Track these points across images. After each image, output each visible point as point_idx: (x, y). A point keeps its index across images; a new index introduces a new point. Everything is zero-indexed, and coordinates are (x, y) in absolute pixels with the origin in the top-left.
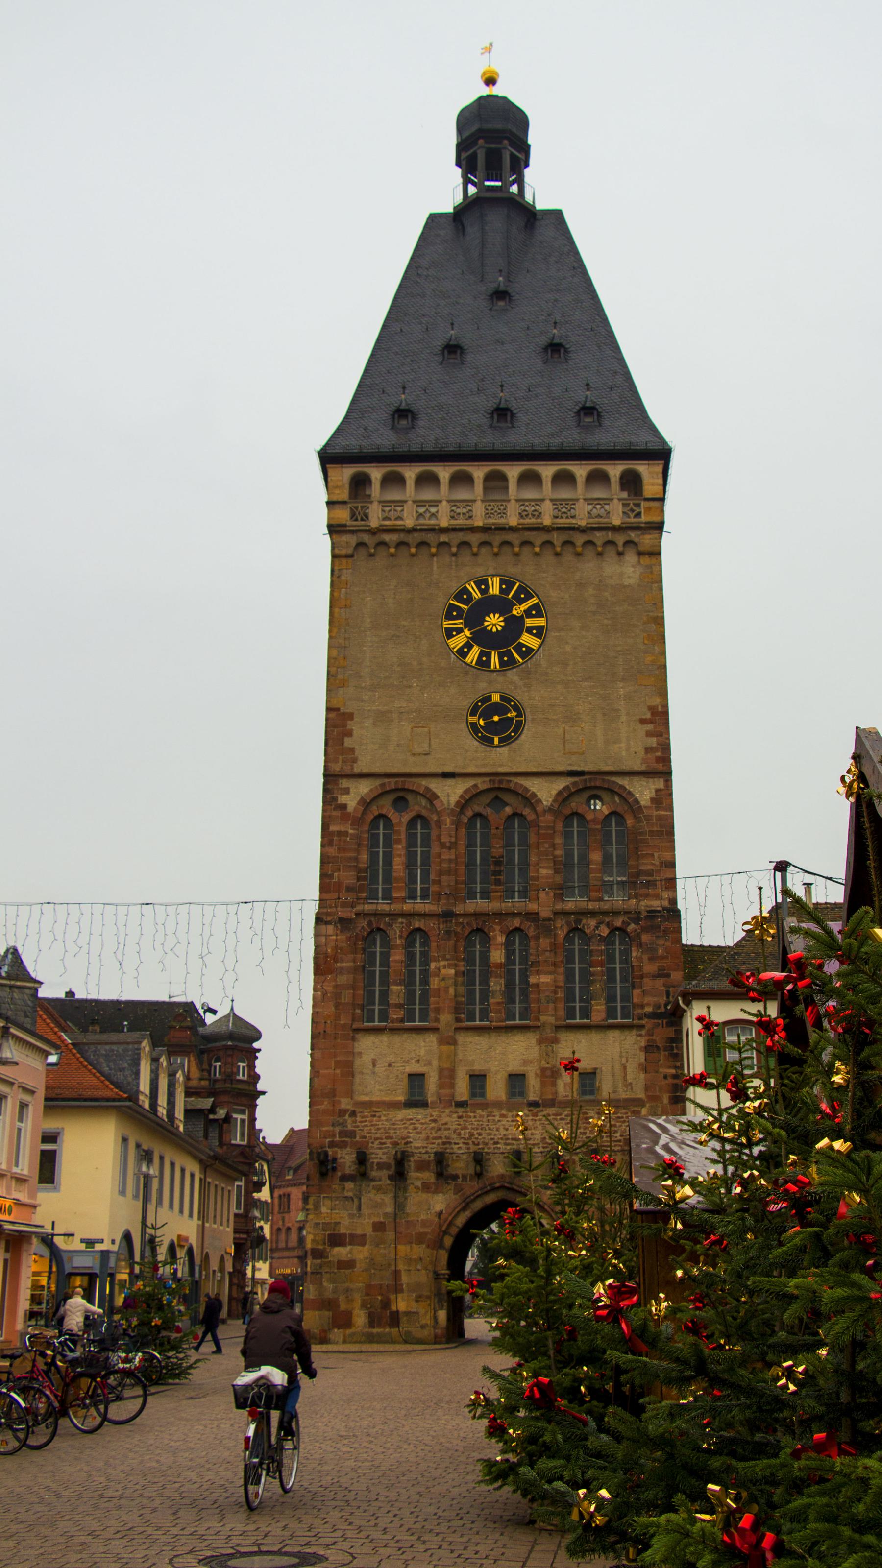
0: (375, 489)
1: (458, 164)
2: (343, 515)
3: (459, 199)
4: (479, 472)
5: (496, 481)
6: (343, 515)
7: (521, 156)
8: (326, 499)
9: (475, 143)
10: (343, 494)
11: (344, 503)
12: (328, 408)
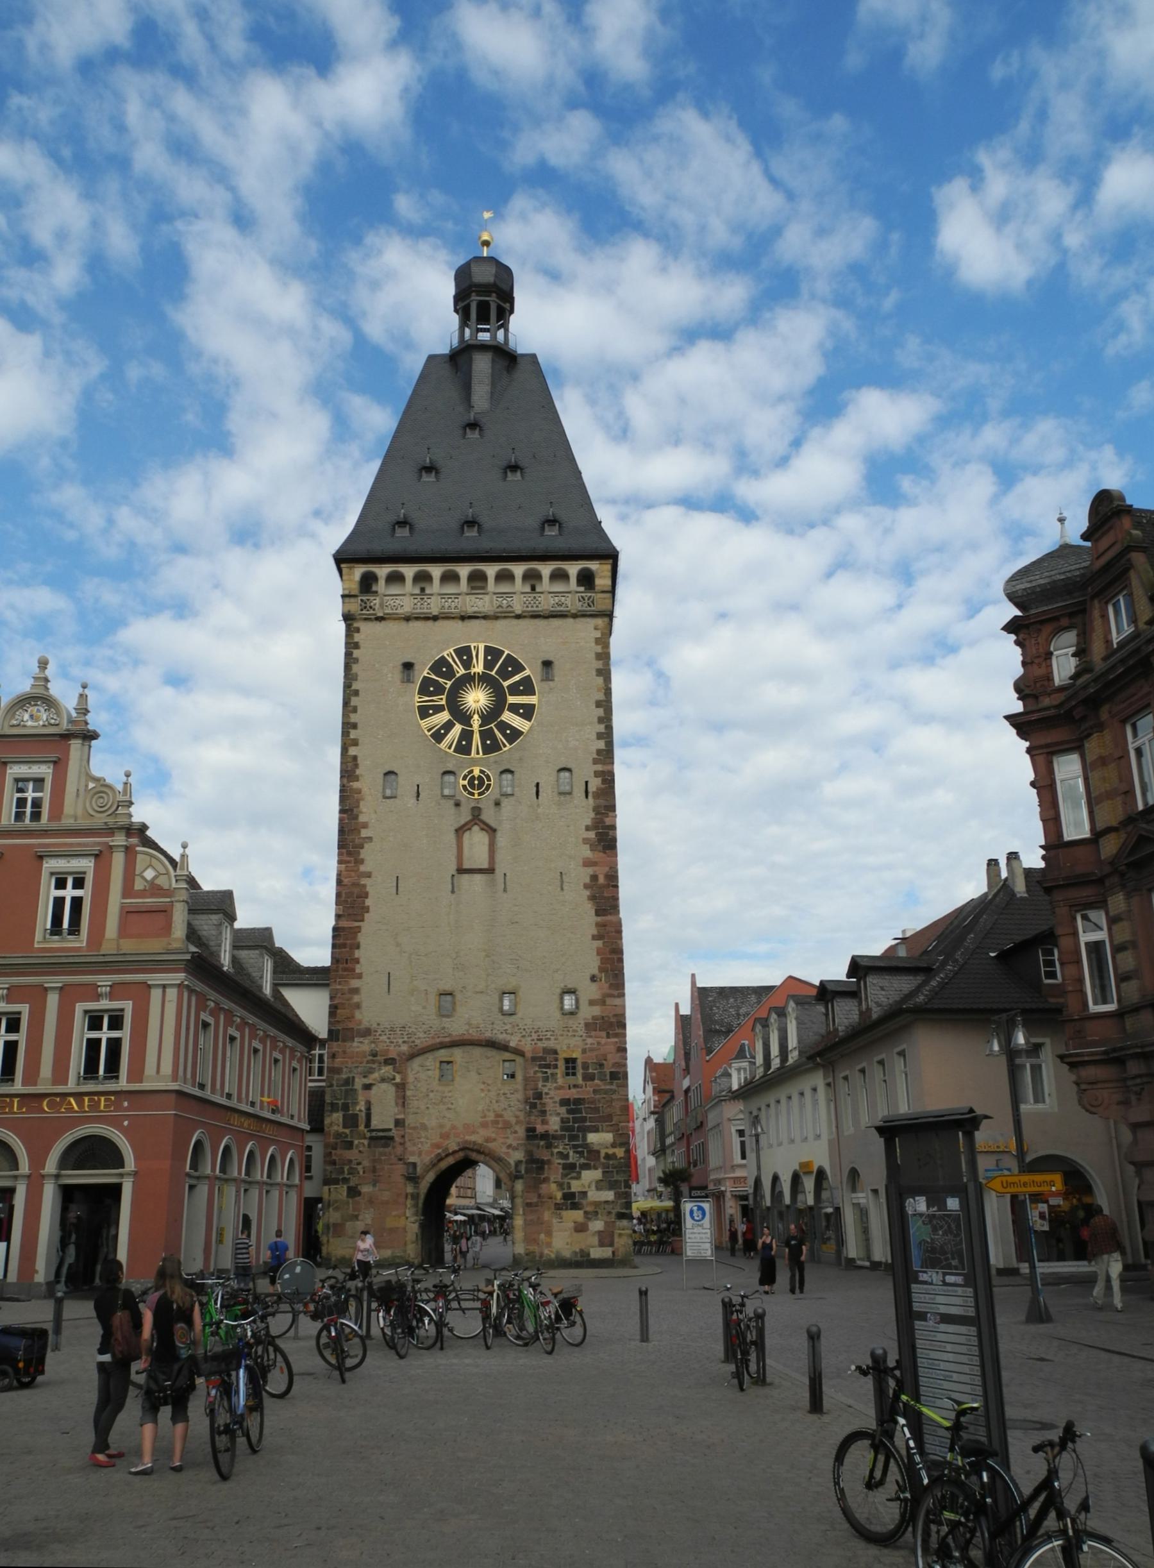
0: (381, 586)
1: (456, 311)
2: (354, 606)
3: (455, 343)
4: (464, 571)
5: (477, 578)
6: (354, 606)
7: (507, 306)
8: (341, 593)
9: (469, 296)
10: (355, 587)
11: (355, 596)
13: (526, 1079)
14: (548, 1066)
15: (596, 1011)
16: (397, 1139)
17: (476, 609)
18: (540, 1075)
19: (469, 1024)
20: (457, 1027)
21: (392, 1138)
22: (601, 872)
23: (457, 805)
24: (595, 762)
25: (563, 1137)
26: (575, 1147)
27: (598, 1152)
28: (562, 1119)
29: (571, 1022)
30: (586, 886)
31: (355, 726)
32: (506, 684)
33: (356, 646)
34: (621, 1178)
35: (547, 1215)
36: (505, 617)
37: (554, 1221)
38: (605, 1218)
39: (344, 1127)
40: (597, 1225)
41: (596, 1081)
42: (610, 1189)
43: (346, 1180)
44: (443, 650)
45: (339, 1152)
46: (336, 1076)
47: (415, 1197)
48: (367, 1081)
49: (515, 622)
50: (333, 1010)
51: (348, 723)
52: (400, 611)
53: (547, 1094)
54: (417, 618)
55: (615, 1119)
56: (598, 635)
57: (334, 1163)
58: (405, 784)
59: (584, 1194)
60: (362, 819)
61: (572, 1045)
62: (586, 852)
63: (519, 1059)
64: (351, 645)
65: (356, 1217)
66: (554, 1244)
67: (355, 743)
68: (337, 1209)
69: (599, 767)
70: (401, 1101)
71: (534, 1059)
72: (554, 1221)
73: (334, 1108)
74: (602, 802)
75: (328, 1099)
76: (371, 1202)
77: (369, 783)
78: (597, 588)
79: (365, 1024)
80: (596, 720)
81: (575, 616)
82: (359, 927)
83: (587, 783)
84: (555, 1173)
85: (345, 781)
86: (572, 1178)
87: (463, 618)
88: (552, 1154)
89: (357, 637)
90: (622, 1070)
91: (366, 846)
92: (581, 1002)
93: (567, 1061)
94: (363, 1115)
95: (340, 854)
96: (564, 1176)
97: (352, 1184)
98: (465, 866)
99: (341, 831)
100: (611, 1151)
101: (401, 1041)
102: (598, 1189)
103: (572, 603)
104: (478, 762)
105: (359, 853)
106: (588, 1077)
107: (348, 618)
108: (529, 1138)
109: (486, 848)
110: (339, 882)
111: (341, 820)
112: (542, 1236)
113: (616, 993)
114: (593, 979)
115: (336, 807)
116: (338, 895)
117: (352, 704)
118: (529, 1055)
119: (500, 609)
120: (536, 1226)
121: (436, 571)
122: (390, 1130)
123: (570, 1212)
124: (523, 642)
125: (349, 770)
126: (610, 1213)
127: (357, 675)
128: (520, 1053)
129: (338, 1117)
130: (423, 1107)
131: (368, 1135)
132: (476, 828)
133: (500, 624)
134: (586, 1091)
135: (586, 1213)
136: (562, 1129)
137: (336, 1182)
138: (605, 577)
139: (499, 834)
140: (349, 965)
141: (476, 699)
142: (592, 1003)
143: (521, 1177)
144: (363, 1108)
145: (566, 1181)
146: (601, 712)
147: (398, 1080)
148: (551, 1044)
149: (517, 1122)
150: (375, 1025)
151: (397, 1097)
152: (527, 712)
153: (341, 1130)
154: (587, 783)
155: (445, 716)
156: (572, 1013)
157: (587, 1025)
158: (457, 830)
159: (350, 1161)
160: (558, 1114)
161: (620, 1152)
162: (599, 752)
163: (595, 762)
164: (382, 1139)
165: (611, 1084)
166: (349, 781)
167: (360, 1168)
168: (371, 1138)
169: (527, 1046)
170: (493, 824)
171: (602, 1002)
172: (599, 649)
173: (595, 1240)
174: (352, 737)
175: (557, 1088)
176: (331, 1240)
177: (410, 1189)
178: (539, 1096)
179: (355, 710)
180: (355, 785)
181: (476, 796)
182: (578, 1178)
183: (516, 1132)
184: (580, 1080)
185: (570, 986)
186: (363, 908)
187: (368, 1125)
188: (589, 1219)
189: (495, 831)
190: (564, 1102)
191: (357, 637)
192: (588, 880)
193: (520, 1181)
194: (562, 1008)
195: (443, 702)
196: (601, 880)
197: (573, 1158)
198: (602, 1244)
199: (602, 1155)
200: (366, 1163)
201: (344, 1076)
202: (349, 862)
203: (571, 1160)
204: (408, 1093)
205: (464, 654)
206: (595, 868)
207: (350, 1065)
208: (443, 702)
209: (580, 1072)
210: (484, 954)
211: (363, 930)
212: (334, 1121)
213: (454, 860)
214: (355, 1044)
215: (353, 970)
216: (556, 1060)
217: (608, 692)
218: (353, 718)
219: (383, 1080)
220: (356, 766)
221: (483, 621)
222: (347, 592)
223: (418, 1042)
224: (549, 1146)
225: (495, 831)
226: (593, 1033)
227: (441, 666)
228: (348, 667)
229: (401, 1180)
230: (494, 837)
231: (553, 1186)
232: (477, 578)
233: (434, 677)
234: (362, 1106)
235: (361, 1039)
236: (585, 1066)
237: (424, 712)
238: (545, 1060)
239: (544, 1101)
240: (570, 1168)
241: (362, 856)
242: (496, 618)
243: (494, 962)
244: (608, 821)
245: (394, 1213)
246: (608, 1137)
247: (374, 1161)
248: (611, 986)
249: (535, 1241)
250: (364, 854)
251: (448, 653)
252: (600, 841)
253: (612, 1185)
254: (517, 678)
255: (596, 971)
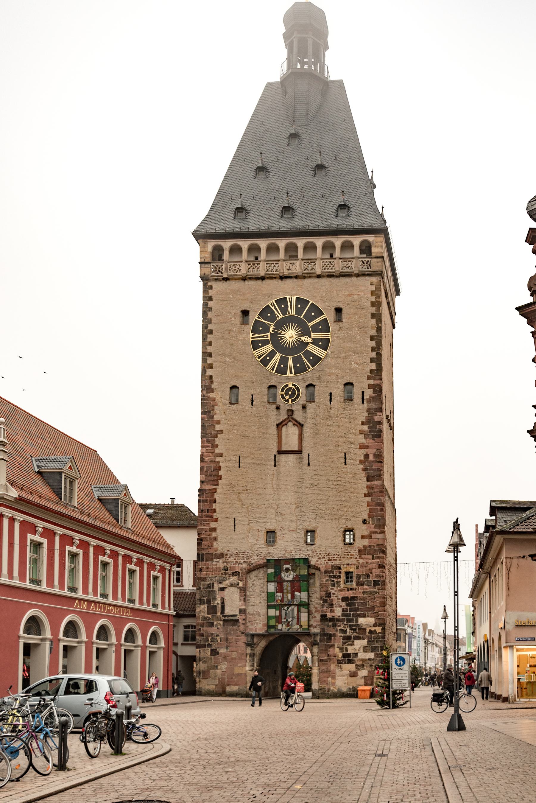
0: (226, 256)
2: (209, 270)
4: (282, 243)
5: (291, 249)
6: (209, 270)
12: (198, 207)
13: (321, 585)
14: (335, 577)
15: (366, 542)
16: (240, 621)
17: (289, 271)
18: (330, 582)
19: (286, 551)
20: (277, 552)
21: (237, 621)
22: (371, 452)
23: (278, 408)
24: (369, 378)
25: (343, 620)
26: (350, 626)
27: (365, 629)
28: (343, 610)
29: (349, 549)
30: (361, 462)
31: (210, 355)
32: (310, 324)
33: (211, 299)
34: (379, 645)
35: (333, 667)
36: (310, 277)
37: (337, 670)
38: (368, 668)
39: (208, 614)
40: (363, 673)
41: (365, 586)
42: (372, 652)
43: (210, 645)
44: (268, 301)
45: (205, 628)
46: (202, 583)
47: (252, 655)
48: (222, 586)
49: (317, 280)
50: (200, 542)
51: (206, 353)
52: (239, 273)
53: (334, 594)
54: (251, 279)
55: (376, 609)
56: (373, 288)
57: (202, 635)
58: (244, 395)
59: (356, 654)
60: (216, 418)
61: (350, 563)
62: (362, 439)
63: (317, 573)
64: (207, 299)
65: (216, 667)
66: (337, 683)
67: (211, 367)
68: (204, 662)
69: (371, 382)
70: (242, 598)
71: (326, 572)
72: (337, 670)
73: (201, 602)
74: (373, 406)
75: (198, 597)
76: (225, 658)
77: (221, 394)
78: (372, 254)
79: (220, 551)
80: (370, 349)
81: (357, 275)
82: (216, 489)
83: (363, 392)
84: (338, 641)
85: (205, 392)
86: (348, 645)
87: (282, 278)
88: (336, 631)
89: (211, 293)
90: (382, 579)
91: (219, 436)
92: (356, 536)
93: (347, 573)
94: (220, 606)
95: (202, 442)
96: (344, 643)
97: (213, 648)
98: (284, 449)
99: (203, 426)
100: (373, 629)
101: (242, 561)
102: (364, 651)
103: (356, 266)
104: (291, 380)
105: (214, 441)
106: (359, 584)
107: (204, 278)
108: (322, 620)
109: (296, 438)
110: (202, 460)
111: (202, 418)
112: (330, 679)
113: (378, 531)
114: (364, 522)
115: (200, 411)
116: (202, 468)
117: (208, 340)
118: (323, 570)
119: (306, 271)
120: (326, 673)
121: (263, 244)
122: (236, 615)
123: (347, 665)
124: (323, 295)
125: (207, 385)
126: (371, 666)
127: (211, 320)
128: (318, 569)
129: (204, 608)
130: (258, 602)
131: (223, 618)
132: (290, 424)
133: (307, 282)
134: (359, 592)
135: (356, 665)
136: (343, 615)
137: (204, 646)
138: (378, 246)
139: (305, 428)
140: (209, 513)
141: (290, 335)
142: (363, 537)
143: (317, 644)
144: (219, 602)
145: (345, 646)
146: (373, 344)
147: (241, 585)
148: (337, 563)
149: (315, 612)
150: (226, 551)
151: (241, 596)
152: (325, 344)
153: (206, 615)
154: (363, 392)
155: (269, 348)
156: (350, 544)
157: (360, 551)
158: (278, 425)
159: (212, 634)
160: (341, 606)
161: (379, 629)
162: (371, 371)
163: (369, 378)
164: (232, 621)
165: (374, 587)
166: (207, 393)
167: (218, 638)
168: (225, 621)
169: (322, 563)
170: (301, 422)
171: (370, 537)
172: (373, 299)
173: (362, 681)
174: (208, 362)
175: (340, 591)
176: (202, 680)
177: (249, 651)
178: (329, 595)
179: (210, 344)
180: (211, 395)
181: (290, 403)
182: (352, 645)
183: (315, 617)
184: (355, 586)
185: (349, 527)
186: (218, 477)
187: (223, 612)
188: (359, 669)
189: (302, 425)
190: (344, 599)
191: (211, 293)
192: (362, 458)
193: (316, 646)
194: (344, 541)
195: (269, 338)
196: (371, 458)
197: (349, 633)
198: (366, 684)
199: (368, 631)
200: (222, 635)
201: (208, 583)
202: (208, 447)
203: (348, 634)
204: (248, 593)
205: (282, 302)
206: (367, 450)
207: (211, 576)
208: (269, 338)
209: (355, 579)
210: (294, 506)
211: (218, 491)
212: (202, 610)
213: (275, 444)
214: (214, 563)
215: (212, 516)
216: (340, 573)
217: (379, 329)
218: (209, 349)
219: (231, 585)
220: (212, 382)
221: (295, 280)
222: (203, 260)
223: (253, 562)
224: (335, 626)
225: (302, 425)
226: (363, 556)
227: (266, 312)
228: (205, 314)
229: (244, 646)
230: (302, 430)
231: (337, 650)
232: (291, 249)
233: (263, 320)
234: (219, 601)
235: (218, 560)
236: (358, 577)
237: (255, 345)
238: (333, 573)
239: (332, 598)
240: (347, 639)
241: (216, 443)
242: (304, 277)
243: (301, 511)
244: (376, 418)
245: (239, 665)
246: (372, 620)
247: (227, 634)
248: (376, 526)
249: (325, 682)
250: (217, 441)
251: (271, 302)
252: (370, 432)
253: (373, 650)
254: (317, 320)
255: (366, 517)
